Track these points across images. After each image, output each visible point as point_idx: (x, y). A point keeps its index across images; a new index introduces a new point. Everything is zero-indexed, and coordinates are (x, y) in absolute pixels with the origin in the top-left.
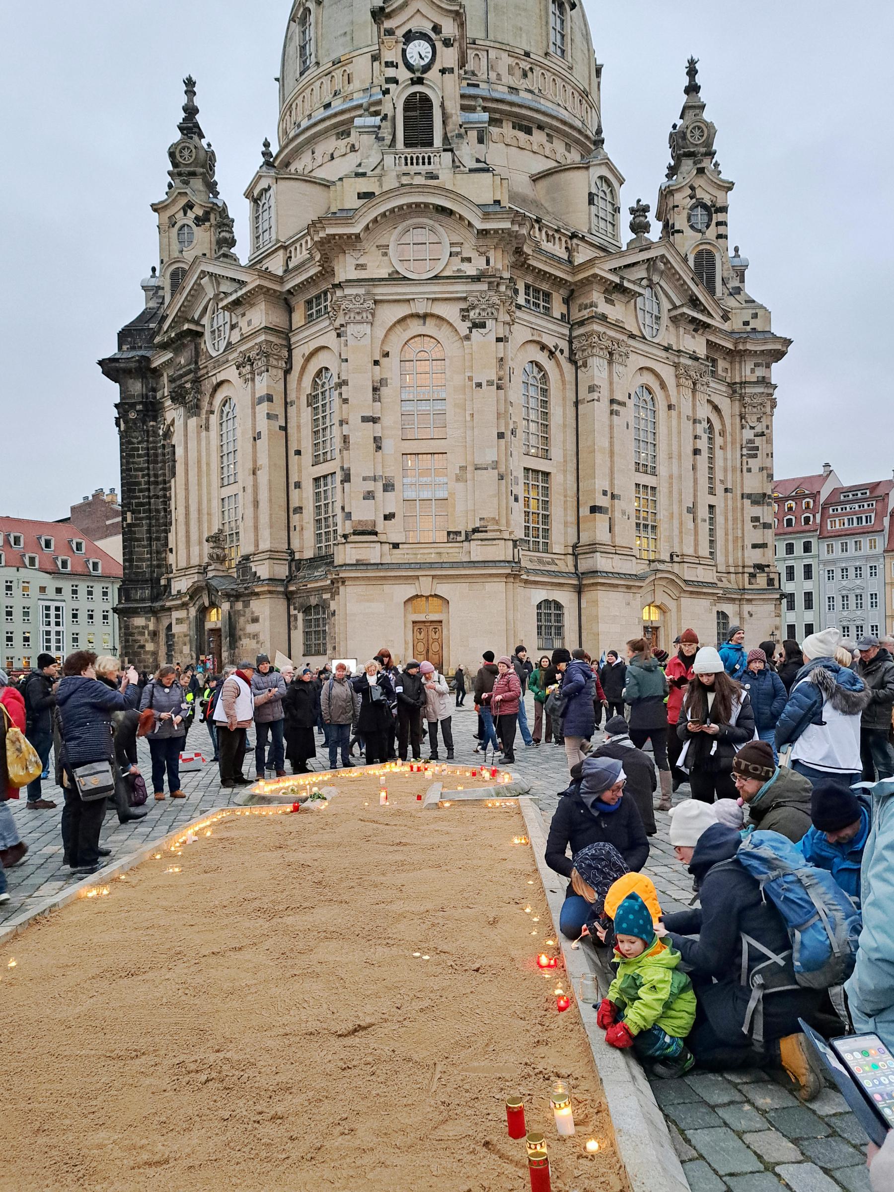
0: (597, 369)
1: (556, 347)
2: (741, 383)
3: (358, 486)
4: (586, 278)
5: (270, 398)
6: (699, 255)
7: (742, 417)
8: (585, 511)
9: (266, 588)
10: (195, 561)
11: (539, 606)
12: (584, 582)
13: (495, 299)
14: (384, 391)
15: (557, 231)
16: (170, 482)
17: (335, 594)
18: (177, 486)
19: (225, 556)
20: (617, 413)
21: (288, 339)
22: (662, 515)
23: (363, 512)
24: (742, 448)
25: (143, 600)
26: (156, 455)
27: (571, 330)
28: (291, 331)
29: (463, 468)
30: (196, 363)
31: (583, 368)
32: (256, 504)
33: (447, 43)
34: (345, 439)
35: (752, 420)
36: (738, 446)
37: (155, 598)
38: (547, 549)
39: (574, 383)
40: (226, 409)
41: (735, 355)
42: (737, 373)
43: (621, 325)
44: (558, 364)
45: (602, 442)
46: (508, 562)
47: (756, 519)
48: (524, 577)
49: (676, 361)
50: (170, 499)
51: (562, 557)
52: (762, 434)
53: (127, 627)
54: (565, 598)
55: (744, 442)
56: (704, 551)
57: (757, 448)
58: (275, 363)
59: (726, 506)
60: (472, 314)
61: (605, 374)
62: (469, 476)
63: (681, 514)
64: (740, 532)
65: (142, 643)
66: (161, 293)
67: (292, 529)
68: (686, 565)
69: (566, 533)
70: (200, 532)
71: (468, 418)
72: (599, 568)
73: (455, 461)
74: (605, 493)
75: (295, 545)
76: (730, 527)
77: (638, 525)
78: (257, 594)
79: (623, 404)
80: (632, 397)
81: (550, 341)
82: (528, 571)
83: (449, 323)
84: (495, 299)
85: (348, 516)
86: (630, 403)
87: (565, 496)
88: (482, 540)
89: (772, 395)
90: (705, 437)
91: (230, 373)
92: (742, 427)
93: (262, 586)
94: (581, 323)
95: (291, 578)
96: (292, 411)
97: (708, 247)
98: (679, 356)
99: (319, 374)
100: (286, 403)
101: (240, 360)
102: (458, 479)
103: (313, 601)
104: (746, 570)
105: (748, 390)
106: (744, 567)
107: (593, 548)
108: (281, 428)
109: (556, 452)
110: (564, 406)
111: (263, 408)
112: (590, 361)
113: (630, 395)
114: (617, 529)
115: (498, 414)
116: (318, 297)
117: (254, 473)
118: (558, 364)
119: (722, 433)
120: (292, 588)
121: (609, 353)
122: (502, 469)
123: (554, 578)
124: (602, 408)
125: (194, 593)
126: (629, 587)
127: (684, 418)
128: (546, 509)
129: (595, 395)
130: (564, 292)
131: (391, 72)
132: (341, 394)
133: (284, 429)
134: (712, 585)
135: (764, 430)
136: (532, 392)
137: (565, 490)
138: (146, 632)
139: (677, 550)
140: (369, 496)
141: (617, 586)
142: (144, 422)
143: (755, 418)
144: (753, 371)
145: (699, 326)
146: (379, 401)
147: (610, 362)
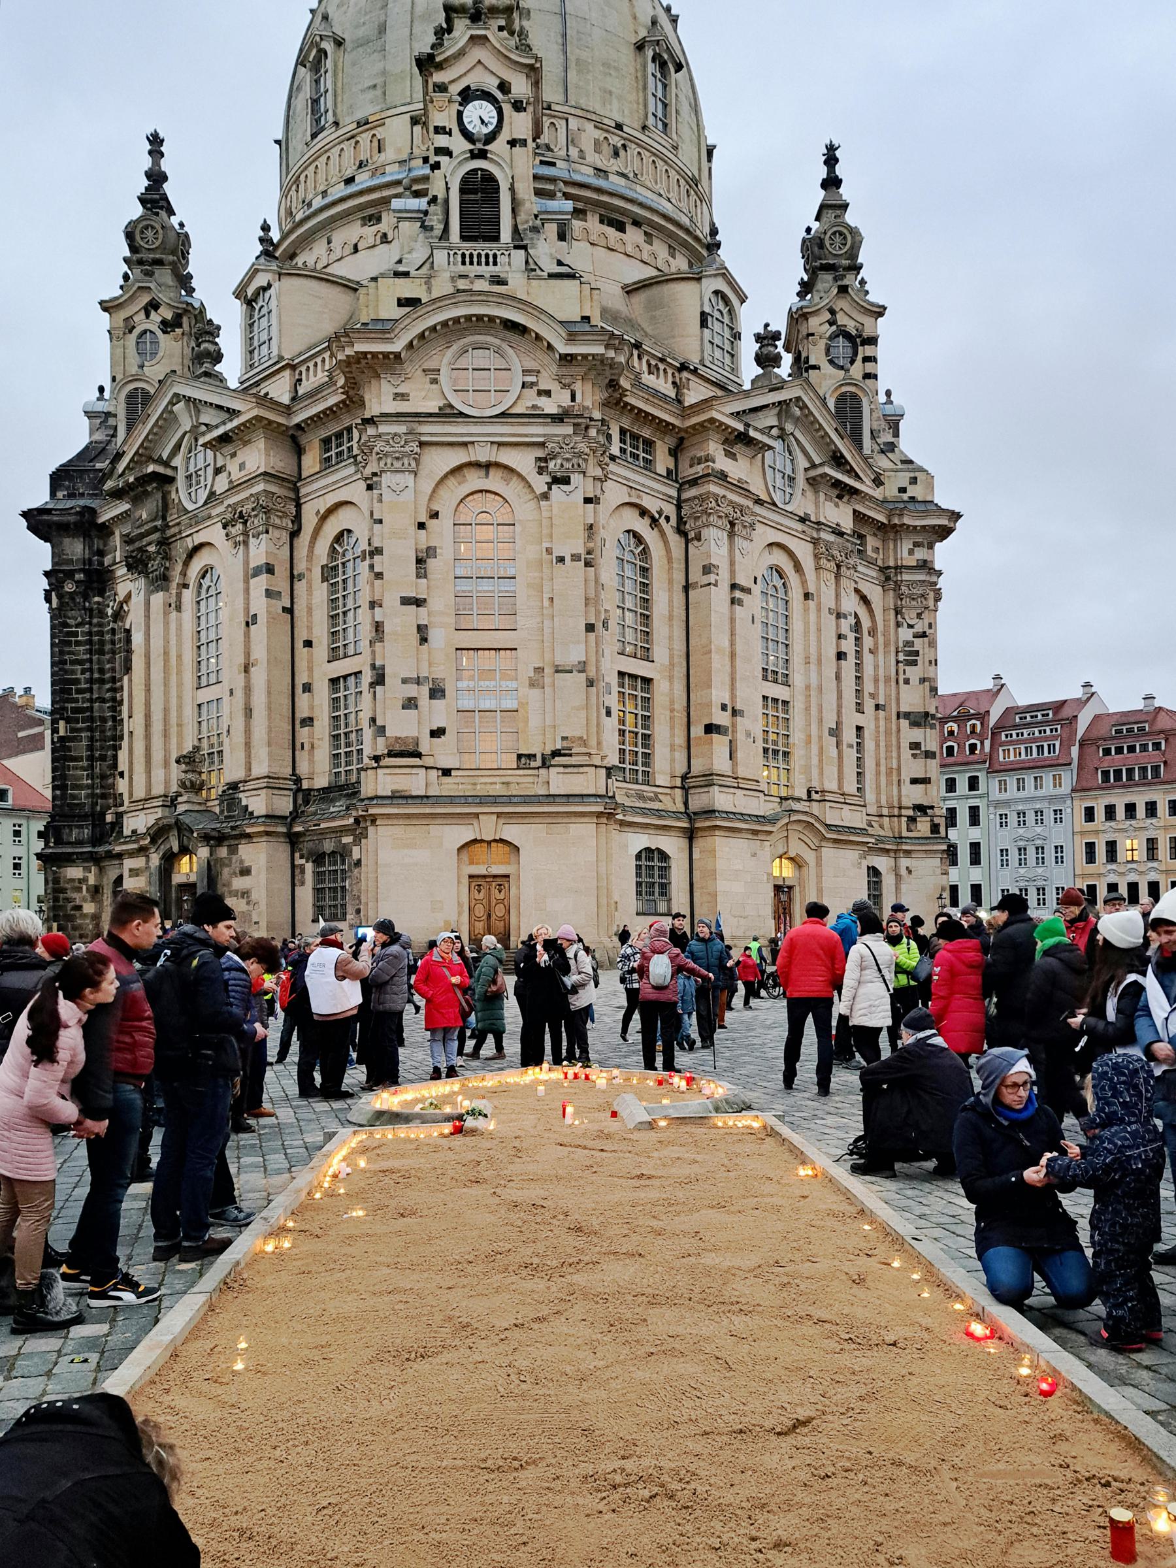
0: (714, 543)
1: (660, 513)
2: (896, 568)
3: (394, 690)
4: (701, 424)
5: (270, 569)
6: (842, 399)
7: (898, 612)
8: (698, 731)
9: (262, 829)
10: (158, 790)
11: (638, 857)
12: (697, 825)
13: (583, 447)
14: (431, 563)
15: (662, 360)
16: (121, 680)
17: (360, 837)
18: (134, 686)
19: (202, 784)
20: (740, 602)
21: (297, 490)
22: (797, 737)
23: (402, 725)
24: (897, 652)
25: (79, 843)
26: (102, 643)
27: (679, 491)
28: (300, 479)
29: (539, 670)
30: (164, 518)
31: (695, 543)
32: (248, 712)
33: (518, 106)
34: (378, 627)
35: (910, 616)
36: (893, 649)
37: (98, 839)
38: (648, 779)
39: (683, 561)
40: (206, 582)
41: (889, 531)
42: (891, 553)
43: (744, 486)
44: (662, 534)
45: (720, 640)
46: (599, 796)
47: (915, 746)
48: (619, 817)
49: (815, 536)
50: (121, 703)
51: (668, 791)
52: (924, 635)
53: (56, 881)
54: (672, 845)
55: (901, 645)
56: (851, 787)
57: (917, 653)
58: (278, 521)
59: (877, 727)
60: (551, 465)
61: (724, 550)
62: (547, 680)
63: (820, 738)
64: (895, 762)
65: (78, 902)
66: (111, 421)
67: (298, 746)
68: (828, 804)
69: (673, 760)
70: (167, 751)
71: (546, 603)
72: (717, 807)
73: (528, 660)
74: (724, 707)
75: (303, 769)
76: (883, 755)
77: (766, 750)
78: (249, 836)
79: (747, 591)
80: (758, 581)
83: (519, 475)
84: (583, 447)
85: (382, 730)
86: (757, 590)
87: (672, 710)
88: (565, 766)
89: (935, 584)
90: (851, 636)
91: (214, 533)
92: (898, 625)
93: (259, 825)
94: (694, 482)
95: (295, 815)
96: (300, 586)
97: (852, 389)
98: (818, 530)
99: (339, 538)
100: (292, 576)
101: (229, 516)
102: (532, 685)
103: (328, 846)
104: (904, 812)
105: (906, 577)
106: (900, 808)
107: (709, 779)
108: (284, 609)
109: (660, 652)
110: (670, 590)
111: (260, 583)
112: (705, 533)
113: (756, 578)
114: (740, 755)
115: (586, 599)
116: (339, 435)
117: (246, 669)
118: (662, 534)
119: (873, 632)
120: (298, 829)
121: (730, 522)
122: (592, 673)
124: (720, 596)
125: (158, 833)
126: (755, 832)
127: (825, 612)
128: (647, 727)
129: (712, 578)
130: (671, 441)
131: (442, 141)
132: (372, 567)
133: (290, 611)
134: (862, 831)
135: (926, 629)
136: (629, 572)
137: (672, 702)
138: (84, 888)
139: (816, 784)
141: (740, 830)
142: (86, 598)
143: (913, 614)
144: (911, 552)
145: (844, 492)
146: (425, 577)
147: (732, 535)
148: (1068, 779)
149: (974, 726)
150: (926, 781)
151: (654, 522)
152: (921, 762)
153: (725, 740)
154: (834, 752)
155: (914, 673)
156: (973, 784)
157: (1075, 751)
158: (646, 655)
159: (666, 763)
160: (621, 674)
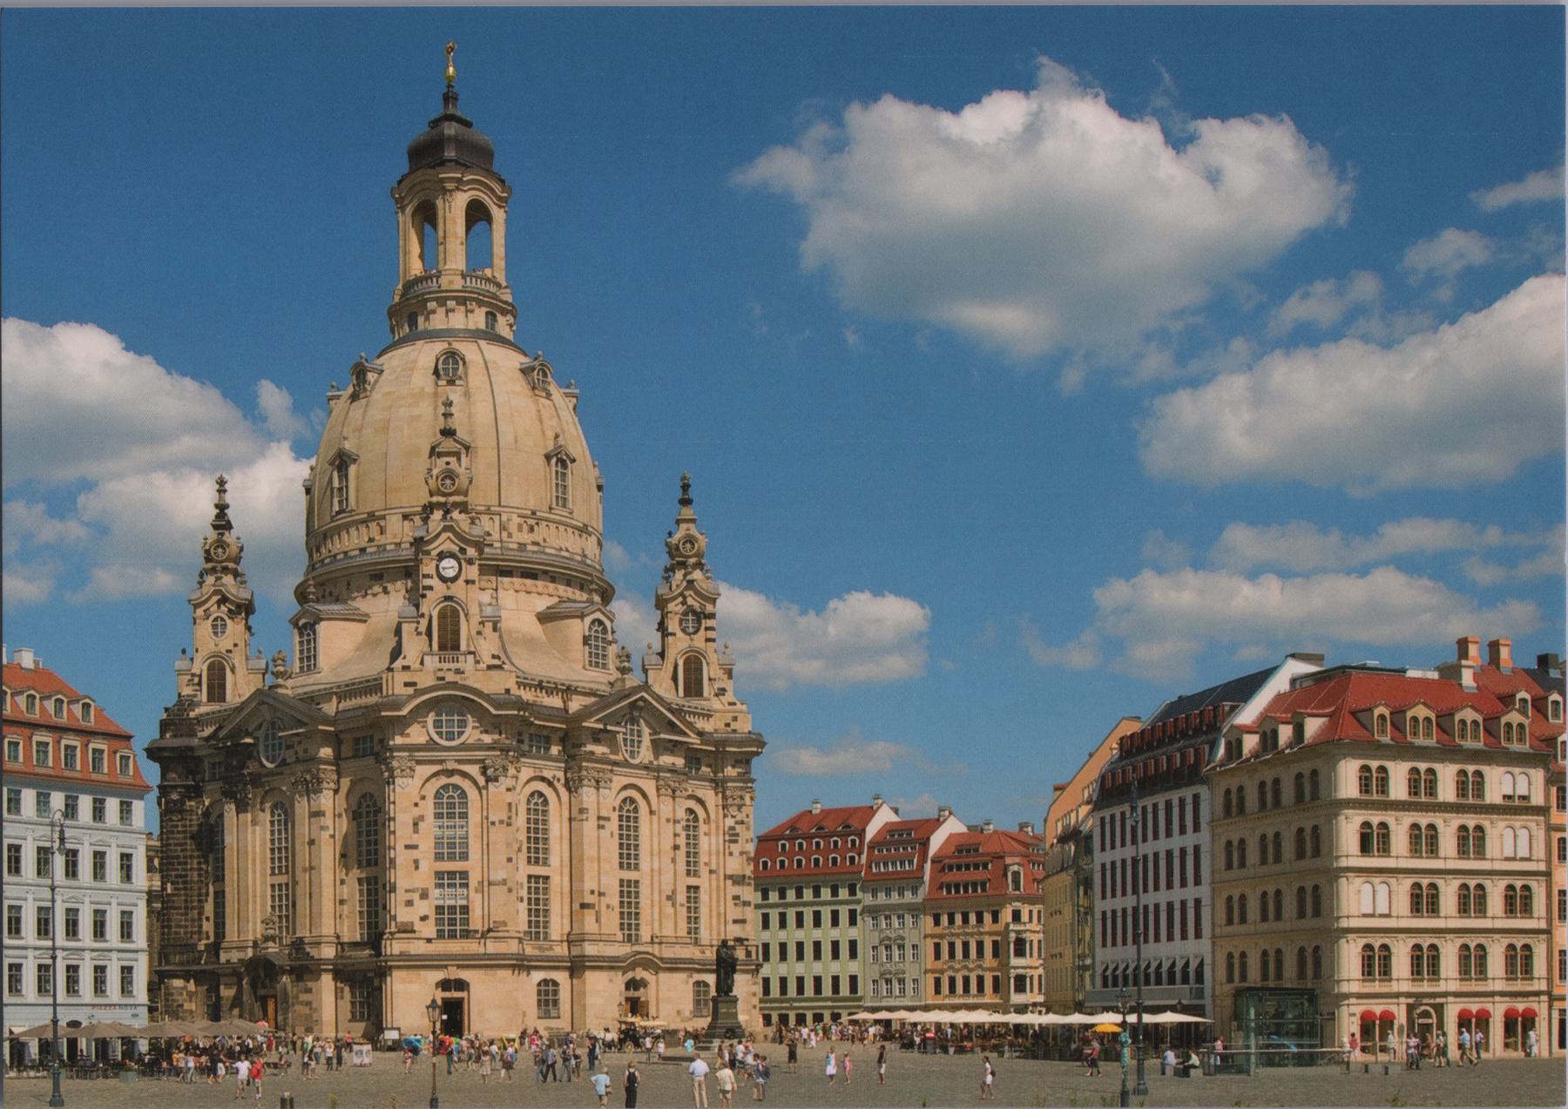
0: (588, 795)
8: (576, 906)
22: (644, 901)
34: (393, 861)
35: (733, 811)
47: (736, 898)
61: (593, 798)
74: (592, 892)
77: (622, 913)
79: (608, 819)
81: (547, 774)
82: (531, 959)
92: (725, 816)
102: (477, 891)
109: (554, 860)
114: (603, 920)
119: (707, 821)
123: (552, 964)
140: (409, 903)
145: (673, 747)
148: (923, 891)
149: (853, 841)
150: (743, 921)
151: (550, 784)
152: (740, 909)
153: (593, 912)
154: (670, 910)
155: (735, 848)
156: (852, 892)
157: (928, 866)
158: (546, 863)
159: (558, 926)
160: (530, 877)
